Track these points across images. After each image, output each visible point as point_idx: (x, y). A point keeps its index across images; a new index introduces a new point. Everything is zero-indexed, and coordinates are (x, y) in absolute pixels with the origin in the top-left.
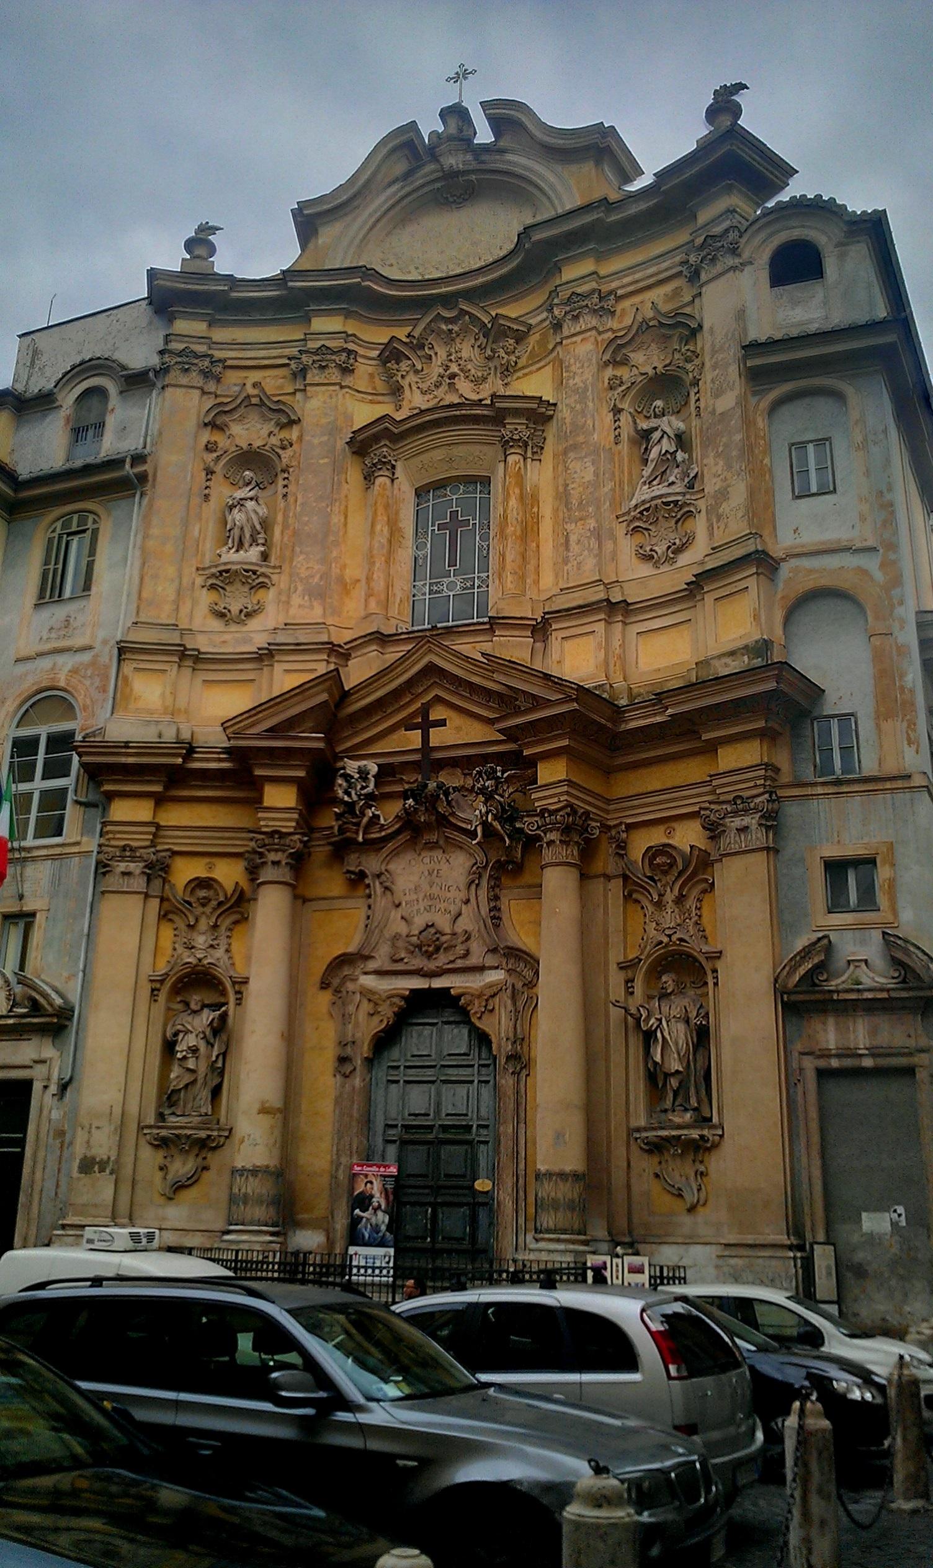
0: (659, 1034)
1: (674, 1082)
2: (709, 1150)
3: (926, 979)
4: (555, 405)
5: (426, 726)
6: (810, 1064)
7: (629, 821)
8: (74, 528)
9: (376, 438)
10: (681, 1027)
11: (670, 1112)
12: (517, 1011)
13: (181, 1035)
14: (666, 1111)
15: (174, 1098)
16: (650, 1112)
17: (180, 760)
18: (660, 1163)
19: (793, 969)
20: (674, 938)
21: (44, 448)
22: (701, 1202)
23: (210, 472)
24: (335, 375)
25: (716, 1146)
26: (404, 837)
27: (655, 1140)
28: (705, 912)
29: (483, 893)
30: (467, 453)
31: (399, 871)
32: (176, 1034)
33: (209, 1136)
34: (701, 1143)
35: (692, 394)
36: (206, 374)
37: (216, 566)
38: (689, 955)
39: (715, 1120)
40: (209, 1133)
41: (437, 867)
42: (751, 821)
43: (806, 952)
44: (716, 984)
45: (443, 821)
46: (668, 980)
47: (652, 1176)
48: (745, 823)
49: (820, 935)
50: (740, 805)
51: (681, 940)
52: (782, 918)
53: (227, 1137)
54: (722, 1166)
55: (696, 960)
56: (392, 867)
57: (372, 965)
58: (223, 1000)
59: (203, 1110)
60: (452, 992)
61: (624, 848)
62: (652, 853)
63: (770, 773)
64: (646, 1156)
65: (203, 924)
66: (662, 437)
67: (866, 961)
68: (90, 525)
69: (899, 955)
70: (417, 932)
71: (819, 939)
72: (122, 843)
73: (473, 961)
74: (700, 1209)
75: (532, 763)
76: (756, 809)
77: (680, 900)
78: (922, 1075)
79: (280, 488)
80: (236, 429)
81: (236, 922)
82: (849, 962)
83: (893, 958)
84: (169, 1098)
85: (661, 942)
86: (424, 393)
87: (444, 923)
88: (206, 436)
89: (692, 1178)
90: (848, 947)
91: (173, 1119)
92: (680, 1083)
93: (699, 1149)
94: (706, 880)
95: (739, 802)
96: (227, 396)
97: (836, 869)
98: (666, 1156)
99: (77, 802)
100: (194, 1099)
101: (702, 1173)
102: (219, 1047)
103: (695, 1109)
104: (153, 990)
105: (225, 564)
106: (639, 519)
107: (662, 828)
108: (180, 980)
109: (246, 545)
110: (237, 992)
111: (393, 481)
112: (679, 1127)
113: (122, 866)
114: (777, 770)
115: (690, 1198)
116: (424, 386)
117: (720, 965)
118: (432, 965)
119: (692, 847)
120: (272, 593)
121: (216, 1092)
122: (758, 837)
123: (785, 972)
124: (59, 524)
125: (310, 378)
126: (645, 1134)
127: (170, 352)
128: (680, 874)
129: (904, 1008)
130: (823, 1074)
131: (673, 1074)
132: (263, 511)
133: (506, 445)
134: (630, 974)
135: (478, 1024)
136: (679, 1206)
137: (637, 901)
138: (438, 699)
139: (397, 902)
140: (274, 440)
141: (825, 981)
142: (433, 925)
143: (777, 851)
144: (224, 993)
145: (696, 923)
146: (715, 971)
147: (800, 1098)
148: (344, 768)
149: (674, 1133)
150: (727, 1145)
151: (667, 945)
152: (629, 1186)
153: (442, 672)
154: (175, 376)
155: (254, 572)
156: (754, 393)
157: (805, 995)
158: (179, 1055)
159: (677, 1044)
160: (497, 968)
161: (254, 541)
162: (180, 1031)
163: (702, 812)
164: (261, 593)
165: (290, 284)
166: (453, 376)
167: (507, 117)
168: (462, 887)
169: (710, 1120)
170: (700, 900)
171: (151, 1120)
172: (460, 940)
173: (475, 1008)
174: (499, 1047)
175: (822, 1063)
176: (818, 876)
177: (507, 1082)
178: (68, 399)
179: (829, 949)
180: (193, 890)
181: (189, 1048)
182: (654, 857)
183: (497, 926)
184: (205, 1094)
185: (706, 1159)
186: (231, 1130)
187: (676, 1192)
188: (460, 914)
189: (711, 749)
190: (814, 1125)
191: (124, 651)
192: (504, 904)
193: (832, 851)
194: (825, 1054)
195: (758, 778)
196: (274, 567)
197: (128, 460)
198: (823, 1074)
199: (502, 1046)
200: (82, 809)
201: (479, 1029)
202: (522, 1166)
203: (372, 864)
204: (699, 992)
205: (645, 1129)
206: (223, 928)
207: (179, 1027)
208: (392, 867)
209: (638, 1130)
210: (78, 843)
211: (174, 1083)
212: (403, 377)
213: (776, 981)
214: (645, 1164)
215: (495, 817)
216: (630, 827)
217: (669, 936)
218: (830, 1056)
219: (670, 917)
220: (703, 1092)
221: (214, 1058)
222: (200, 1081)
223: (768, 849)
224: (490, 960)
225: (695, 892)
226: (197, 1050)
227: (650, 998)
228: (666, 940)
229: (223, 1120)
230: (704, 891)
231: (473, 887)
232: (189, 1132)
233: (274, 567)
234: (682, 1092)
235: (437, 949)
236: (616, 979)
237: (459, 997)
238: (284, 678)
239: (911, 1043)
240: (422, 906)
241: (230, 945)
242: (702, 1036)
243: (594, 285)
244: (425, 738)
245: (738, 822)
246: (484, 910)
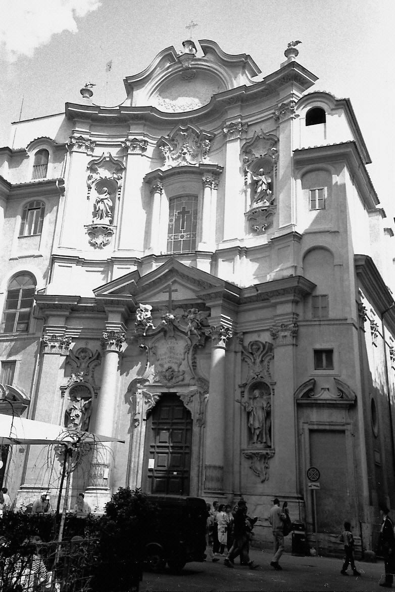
2: (269, 458)
3: (350, 397)
4: (223, 168)
5: (170, 292)
6: (306, 427)
7: (244, 331)
8: (35, 207)
9: (155, 178)
11: (255, 444)
12: (201, 402)
13: (73, 410)
14: (254, 443)
16: (249, 444)
17: (76, 303)
18: (252, 463)
19: (301, 390)
20: (259, 376)
21: (22, 174)
22: (267, 479)
23: (90, 188)
24: (138, 151)
25: (272, 457)
26: (162, 334)
27: (250, 454)
28: (270, 366)
29: (190, 356)
30: (188, 185)
31: (159, 347)
32: (71, 410)
35: (274, 167)
36: (87, 147)
37: (92, 225)
38: (264, 383)
39: (272, 447)
41: (173, 346)
42: (287, 333)
43: (305, 385)
44: (274, 395)
45: (176, 328)
46: (257, 393)
48: (285, 334)
49: (312, 378)
50: (284, 327)
51: (262, 377)
52: (297, 369)
55: (267, 385)
56: (156, 345)
57: (147, 383)
58: (89, 396)
60: (177, 394)
61: (242, 341)
62: (252, 344)
63: (295, 316)
64: (247, 460)
65: (83, 365)
66: (262, 184)
67: (328, 389)
68: (41, 206)
69: (340, 387)
70: (164, 371)
71: (311, 380)
72: (52, 334)
73: (186, 382)
74: (266, 482)
75: (209, 309)
76: (289, 330)
77: (262, 361)
78: (347, 433)
79: (117, 195)
80: (100, 170)
81: (96, 366)
82: (322, 389)
83: (338, 388)
85: (254, 378)
86: (173, 159)
87: (175, 367)
88: (89, 173)
90: (322, 383)
92: (260, 432)
93: (266, 458)
94: (271, 355)
95: (283, 326)
96: (96, 157)
97: (318, 353)
99: (35, 318)
101: (267, 468)
103: (265, 443)
104: (62, 392)
105: (96, 224)
106: (252, 216)
107: (256, 334)
109: (104, 217)
110: (95, 393)
111: (161, 195)
112: (260, 450)
113: (52, 344)
114: (298, 315)
115: (263, 478)
116: (174, 157)
117: (275, 387)
118: (169, 384)
119: (266, 342)
120: (114, 236)
122: (290, 340)
124: (28, 205)
125: (130, 152)
126: (246, 452)
127: (74, 137)
128: (262, 352)
129: (342, 407)
130: (312, 431)
131: (257, 429)
132: (111, 204)
133: (204, 184)
134: (243, 389)
135: (186, 406)
136: (258, 480)
137: (246, 361)
138: (175, 282)
139: (157, 359)
140: (115, 176)
141: (313, 395)
142: (171, 368)
143: (297, 346)
144: (90, 393)
146: (273, 390)
147: (303, 441)
148: (139, 308)
150: (276, 457)
151: (256, 379)
152: (240, 472)
153: (177, 271)
154: (75, 148)
155: (107, 228)
156: (297, 169)
157: (306, 399)
158: (72, 418)
159: (259, 417)
160: (194, 385)
161: (107, 216)
162: (72, 409)
163: (271, 329)
164: (109, 238)
165: (122, 112)
166: (185, 154)
167: (209, 47)
168: (182, 354)
169: (270, 447)
170: (269, 362)
172: (181, 374)
173: (185, 401)
174: (194, 416)
175: (311, 427)
176: (311, 355)
177: (196, 429)
178: (32, 154)
179: (315, 383)
180: (79, 353)
181: (76, 415)
182: (252, 345)
183: (194, 369)
188: (181, 364)
189: (274, 306)
190: (308, 451)
191: (54, 259)
192: (198, 361)
193: (318, 346)
194: (312, 423)
195: (291, 318)
196: (114, 226)
197: (57, 182)
198: (312, 431)
199: (195, 416)
200: (36, 321)
201: (186, 408)
202: (201, 463)
203: (149, 344)
204: (268, 397)
206: (91, 368)
207: (73, 407)
208: (156, 345)
209: (244, 450)
210: (34, 334)
212: (166, 153)
213: (294, 394)
214: (246, 464)
215: (195, 329)
216: (244, 333)
217: (257, 375)
218: (314, 424)
219: (258, 368)
220: (268, 436)
223: (293, 345)
224: (192, 382)
227: (250, 398)
228: (256, 377)
230: (271, 359)
231: (186, 354)
233: (114, 226)
234: (260, 435)
235: (172, 378)
236: (238, 391)
237: (180, 397)
238: (118, 272)
239: (344, 421)
240: (168, 360)
241: (93, 374)
242: (268, 414)
243: (240, 120)
244: (170, 296)
245: (283, 334)
246: (190, 362)
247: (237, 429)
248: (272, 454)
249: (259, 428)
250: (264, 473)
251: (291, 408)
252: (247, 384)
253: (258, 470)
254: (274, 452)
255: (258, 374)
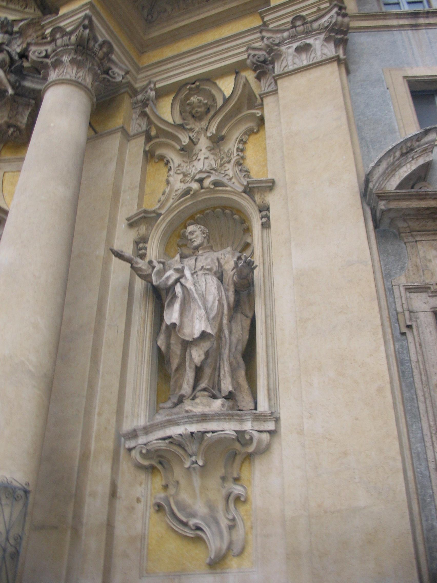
0: (178, 289)
1: (197, 355)
2: (250, 457)
10: (212, 281)
14: (181, 400)
16: (156, 408)
18: (166, 487)
22: (236, 549)
25: (263, 450)
34: (237, 446)
47: (151, 511)
51: (216, 184)
54: (279, 484)
64: (142, 476)
74: (233, 563)
89: (221, 506)
92: (207, 354)
98: (178, 473)
101: (238, 499)
112: (204, 418)
115: (215, 544)
117: (273, 200)
123: (381, 169)
126: (142, 440)
136: (198, 556)
137: (162, 158)
145: (238, 164)
146: (264, 209)
149: (194, 428)
151: (196, 192)
152: (110, 526)
159: (204, 301)
185: (245, 474)
187: (190, 534)
205: (147, 430)
209: (134, 434)
217: (200, 181)
225: (237, 134)
228: (195, 186)
230: (250, 132)
242: (243, 291)
247: (110, 359)
248: (265, 437)
249: (204, 335)
250: (224, 523)
251: (353, 235)
252: (159, 215)
253: (194, 515)
254: (271, 426)
255: (204, 175)
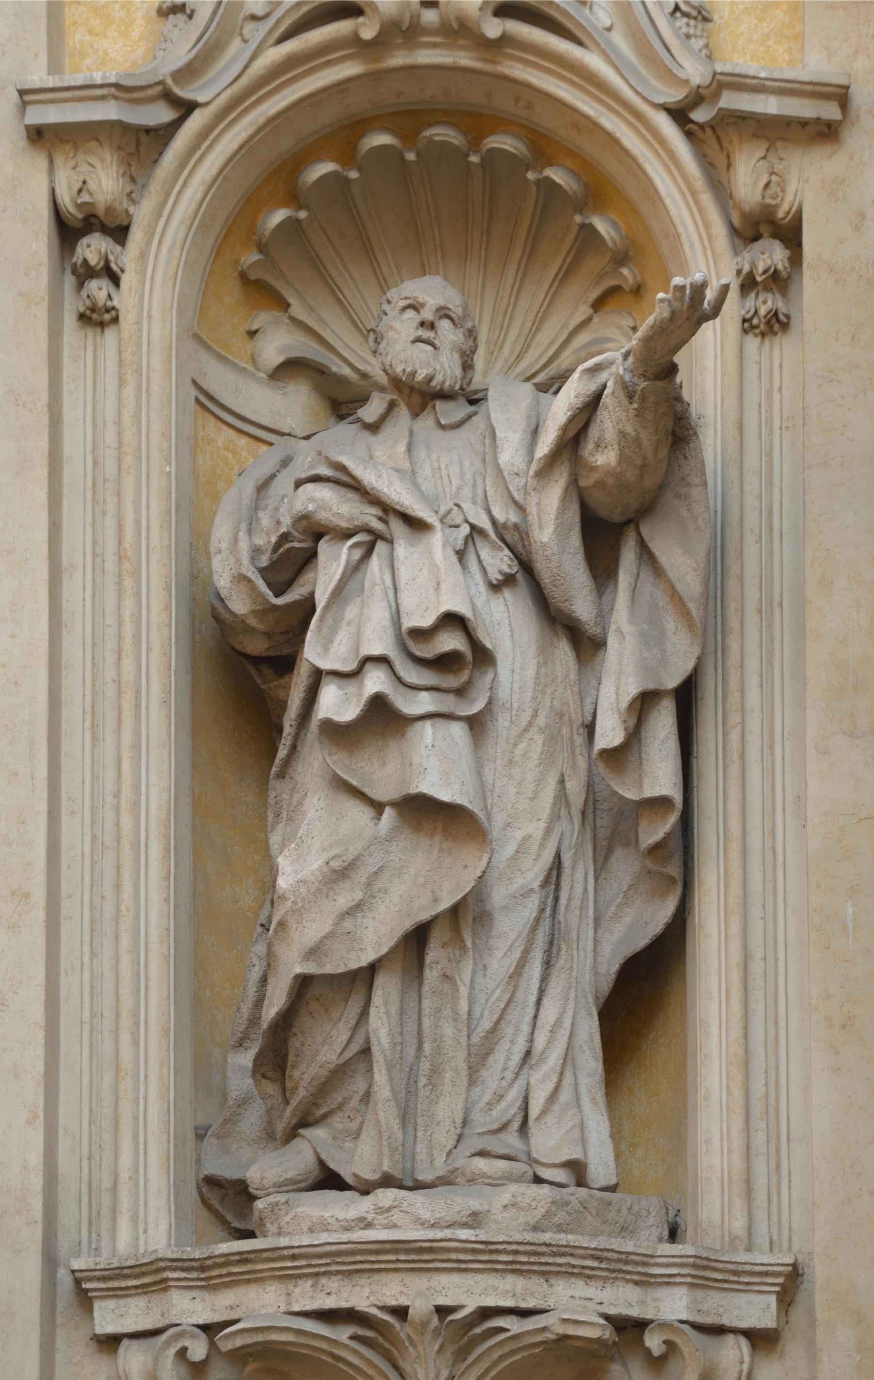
13: (333, 562)
15: (324, 1045)
32: (291, 559)
33: (629, 1329)
40: (625, 1300)
53: (761, 1340)
59: (551, 1142)
84: (284, 1048)
91: (330, 1216)
100: (478, 1059)
102: (652, 638)
104: (68, 230)
108: (274, 171)
121: (641, 998)
158: (337, 704)
171: (150, 1221)
184: (568, 1021)
186: (791, 1284)
207: (331, 504)
211: (311, 929)
221: (610, 733)
222: (512, 924)
226: (482, 656)
229: (716, 1213)
232: (469, 1292)
